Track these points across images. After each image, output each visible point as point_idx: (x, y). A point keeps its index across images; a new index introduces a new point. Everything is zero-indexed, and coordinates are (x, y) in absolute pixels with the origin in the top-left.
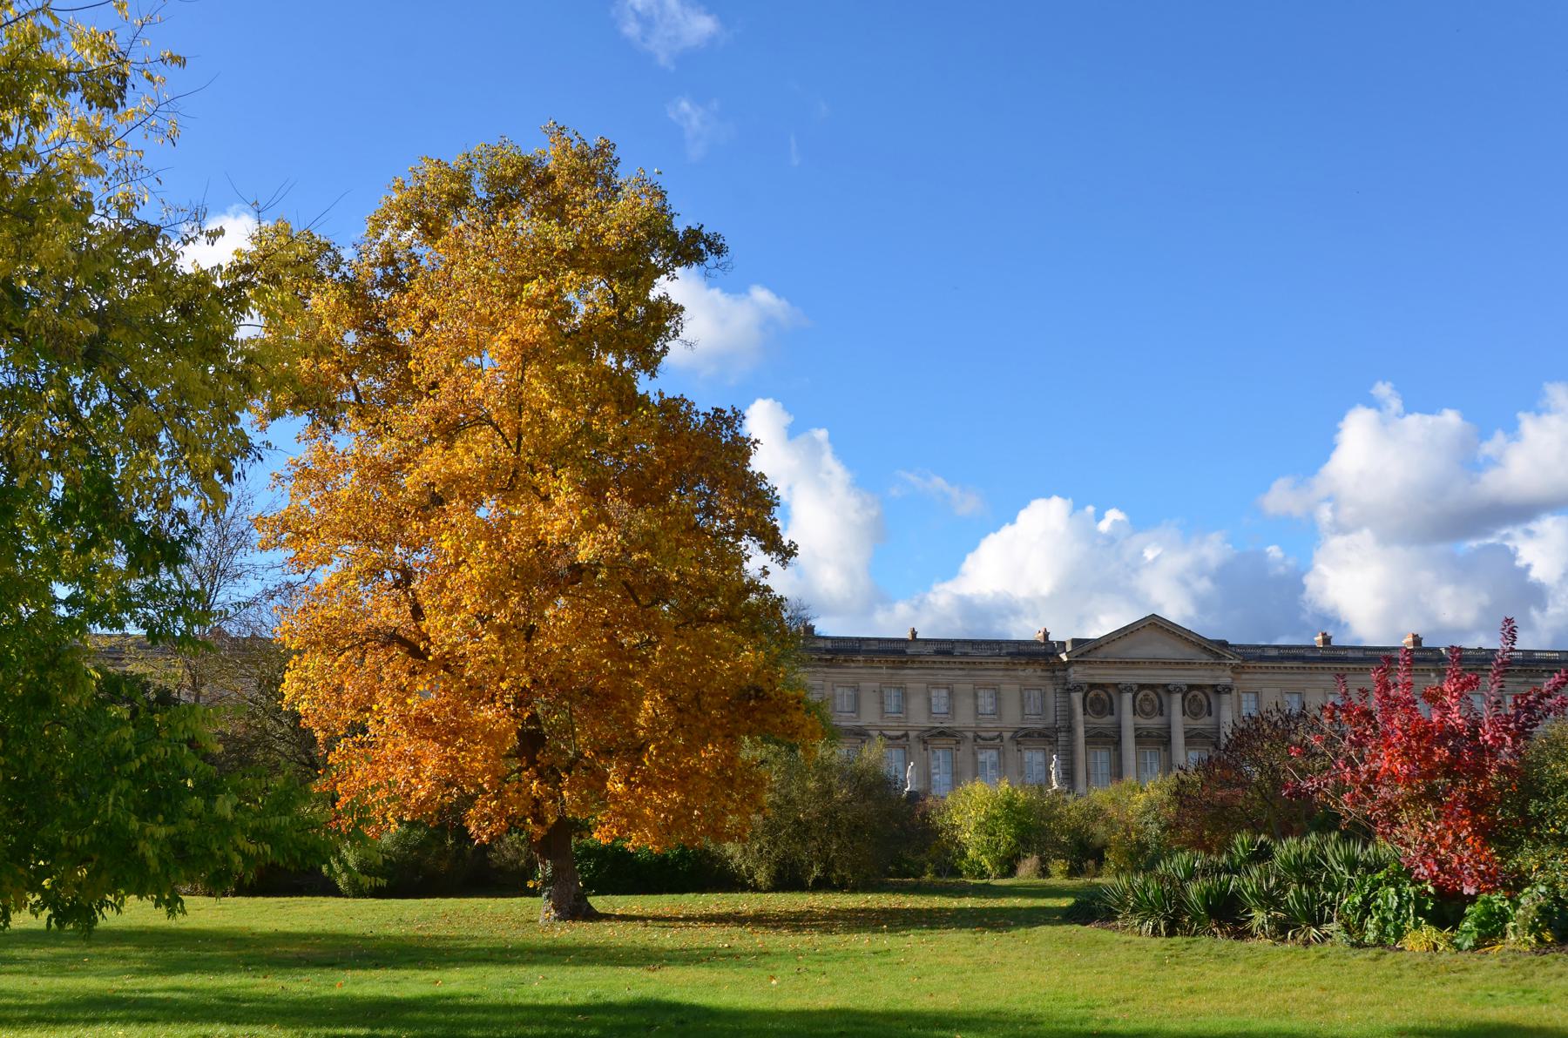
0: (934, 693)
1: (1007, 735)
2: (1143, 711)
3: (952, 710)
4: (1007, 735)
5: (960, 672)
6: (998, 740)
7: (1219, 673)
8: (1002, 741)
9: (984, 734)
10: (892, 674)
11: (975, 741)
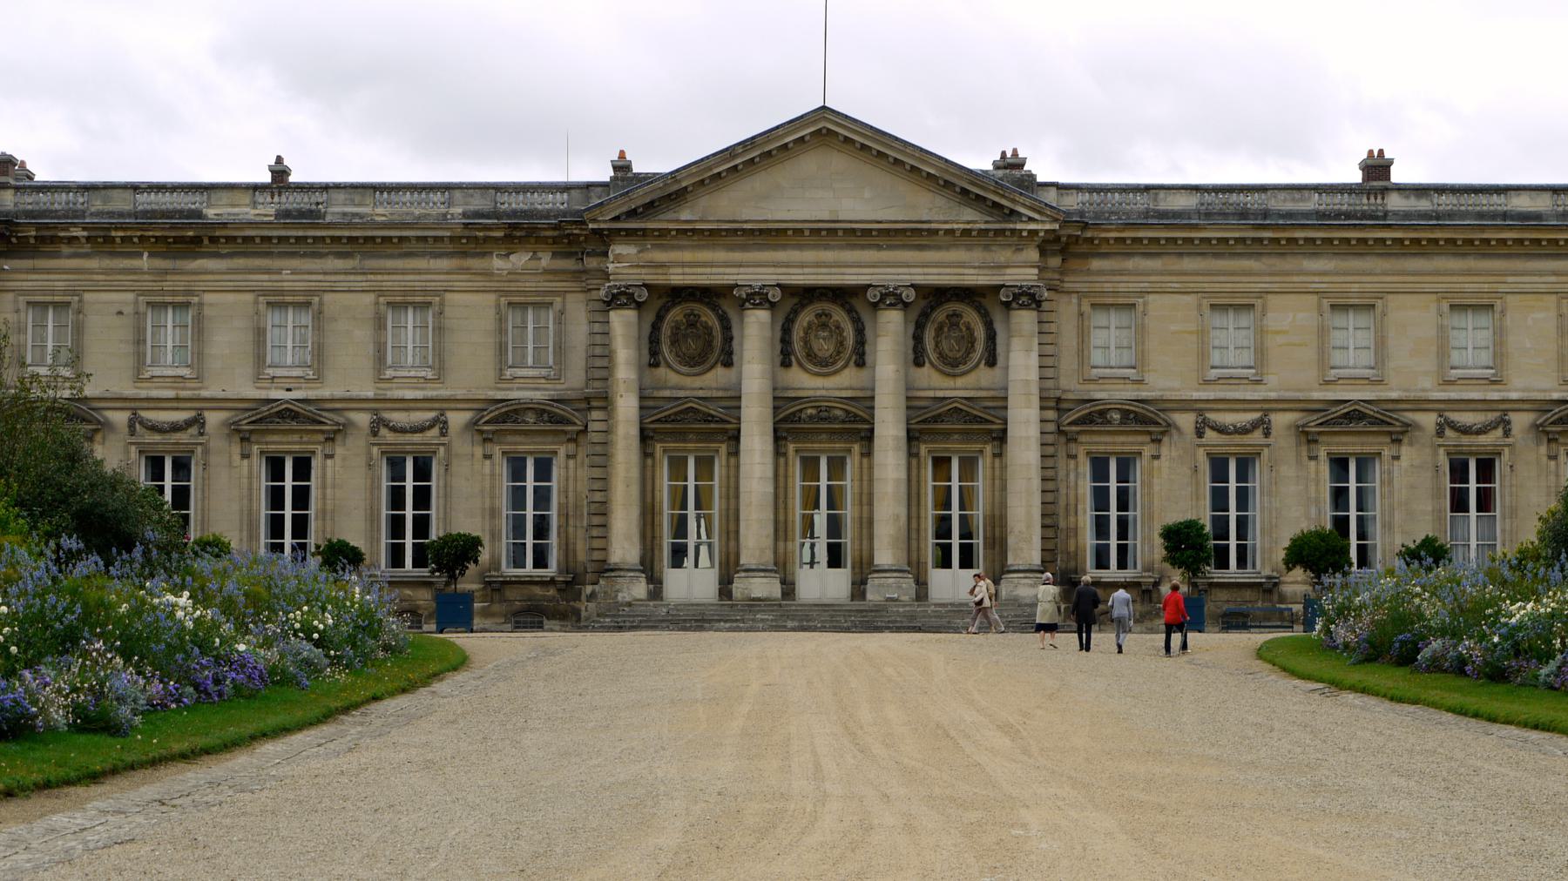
0: (271, 318)
1: (457, 419)
2: (811, 356)
3: (319, 359)
4: (457, 419)
5: (340, 264)
6: (435, 431)
7: (1003, 255)
8: (443, 434)
9: (398, 418)
10: (166, 272)
11: (375, 434)
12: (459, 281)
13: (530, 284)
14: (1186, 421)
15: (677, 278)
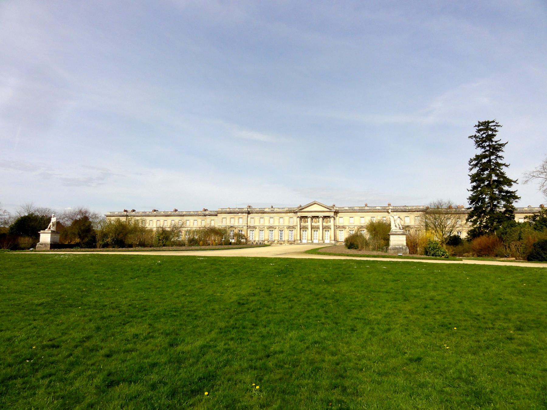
1: (285, 227)
4: (285, 227)
9: (281, 227)
12: (285, 216)
13: (291, 216)
14: (347, 227)
15: (303, 215)
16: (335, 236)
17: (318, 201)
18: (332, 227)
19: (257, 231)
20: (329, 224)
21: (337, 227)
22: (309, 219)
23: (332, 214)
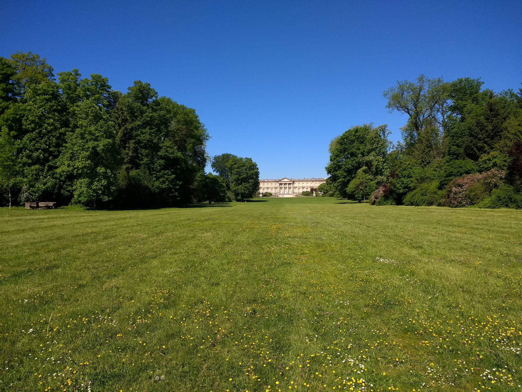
16: (293, 191)
17: (287, 177)
18: (292, 187)
19: (297, 189)
20: (291, 186)
21: (294, 187)
22: (283, 184)
23: (292, 182)
